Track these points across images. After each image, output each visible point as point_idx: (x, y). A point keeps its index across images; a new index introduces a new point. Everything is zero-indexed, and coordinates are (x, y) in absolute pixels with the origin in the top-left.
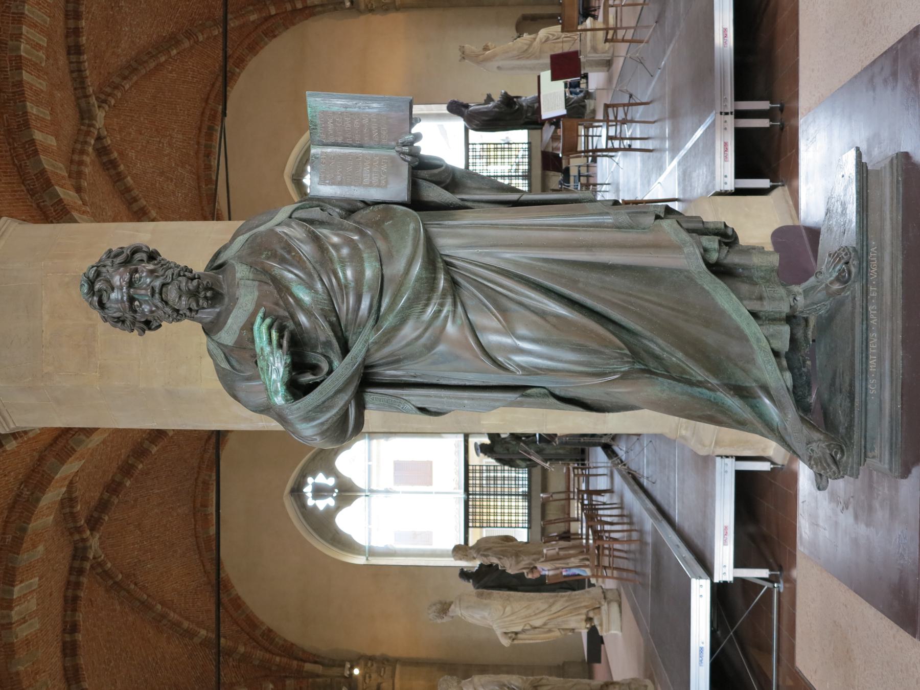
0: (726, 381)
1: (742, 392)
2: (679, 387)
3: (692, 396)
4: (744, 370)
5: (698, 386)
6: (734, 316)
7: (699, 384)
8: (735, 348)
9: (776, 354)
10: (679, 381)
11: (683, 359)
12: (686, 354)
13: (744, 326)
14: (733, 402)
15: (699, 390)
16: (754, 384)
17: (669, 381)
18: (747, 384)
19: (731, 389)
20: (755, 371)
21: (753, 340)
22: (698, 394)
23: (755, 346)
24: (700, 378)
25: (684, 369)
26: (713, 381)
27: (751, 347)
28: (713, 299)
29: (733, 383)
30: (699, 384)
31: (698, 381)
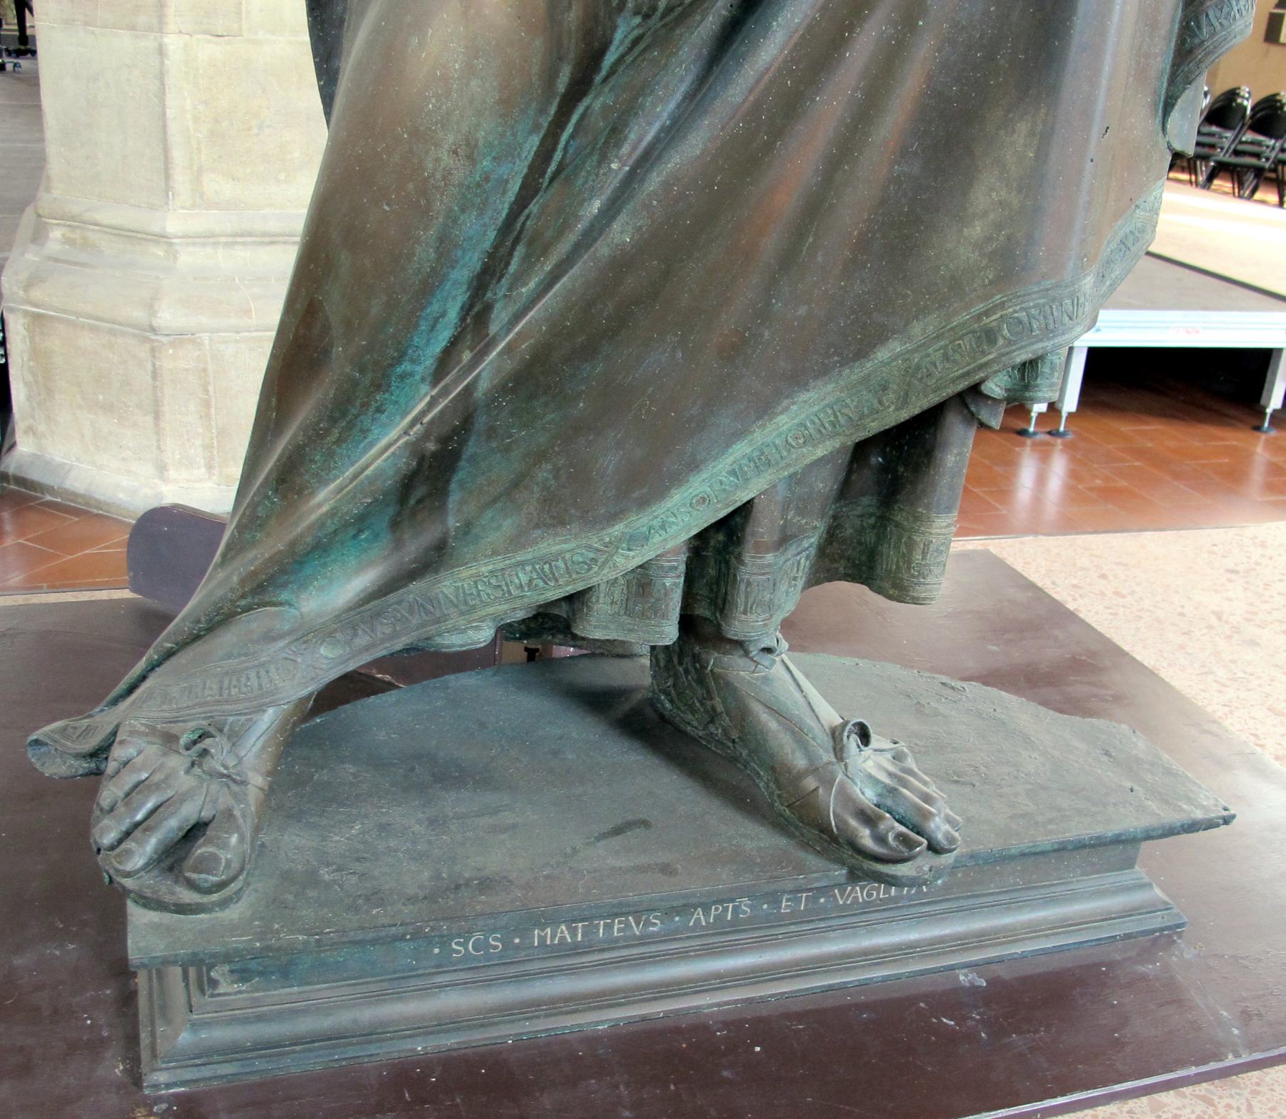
0: (481, 421)
1: (428, 477)
2: (479, 233)
3: (428, 287)
4: (516, 484)
5: (466, 310)
6: (741, 449)
7: (476, 317)
8: (609, 460)
9: (577, 600)
10: (506, 227)
11: (603, 249)
12: (622, 263)
13: (698, 485)
14: (385, 446)
15: (453, 314)
16: (453, 522)
17: (514, 187)
18: (454, 498)
19: (444, 440)
20: (508, 525)
21: (639, 521)
22: (435, 308)
23: (618, 529)
24: (500, 316)
25: (545, 251)
26: (487, 371)
27: (613, 518)
28: (823, 372)
29: (471, 448)
30: (476, 317)
31: (488, 308)
